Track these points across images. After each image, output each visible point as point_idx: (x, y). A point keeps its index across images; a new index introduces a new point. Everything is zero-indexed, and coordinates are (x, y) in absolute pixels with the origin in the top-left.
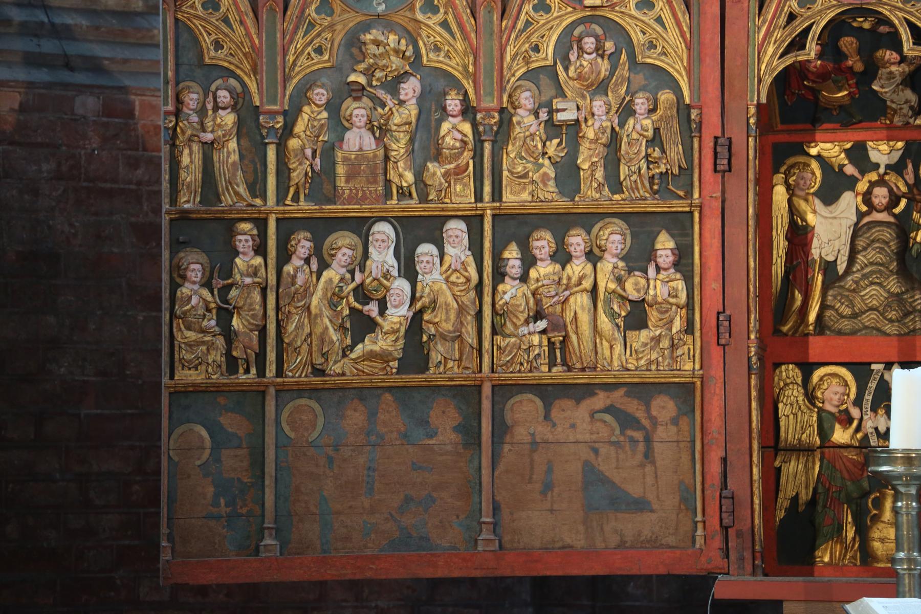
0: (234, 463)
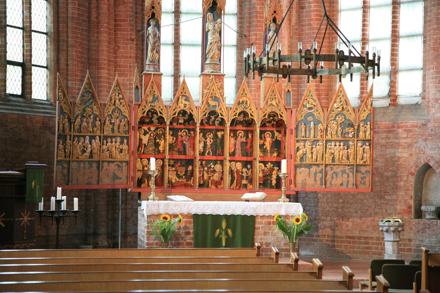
0: (65, 171)
